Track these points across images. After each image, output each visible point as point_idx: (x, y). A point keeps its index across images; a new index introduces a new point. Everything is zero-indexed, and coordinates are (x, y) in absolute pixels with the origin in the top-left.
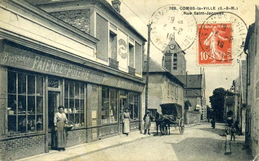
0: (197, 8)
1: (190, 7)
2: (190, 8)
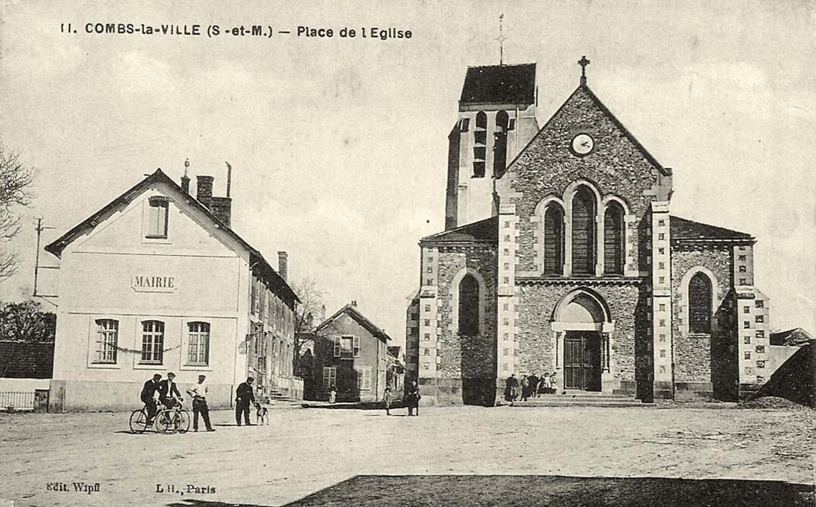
0: (141, 28)
1: (119, 25)
2: (119, 29)
